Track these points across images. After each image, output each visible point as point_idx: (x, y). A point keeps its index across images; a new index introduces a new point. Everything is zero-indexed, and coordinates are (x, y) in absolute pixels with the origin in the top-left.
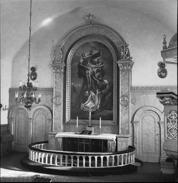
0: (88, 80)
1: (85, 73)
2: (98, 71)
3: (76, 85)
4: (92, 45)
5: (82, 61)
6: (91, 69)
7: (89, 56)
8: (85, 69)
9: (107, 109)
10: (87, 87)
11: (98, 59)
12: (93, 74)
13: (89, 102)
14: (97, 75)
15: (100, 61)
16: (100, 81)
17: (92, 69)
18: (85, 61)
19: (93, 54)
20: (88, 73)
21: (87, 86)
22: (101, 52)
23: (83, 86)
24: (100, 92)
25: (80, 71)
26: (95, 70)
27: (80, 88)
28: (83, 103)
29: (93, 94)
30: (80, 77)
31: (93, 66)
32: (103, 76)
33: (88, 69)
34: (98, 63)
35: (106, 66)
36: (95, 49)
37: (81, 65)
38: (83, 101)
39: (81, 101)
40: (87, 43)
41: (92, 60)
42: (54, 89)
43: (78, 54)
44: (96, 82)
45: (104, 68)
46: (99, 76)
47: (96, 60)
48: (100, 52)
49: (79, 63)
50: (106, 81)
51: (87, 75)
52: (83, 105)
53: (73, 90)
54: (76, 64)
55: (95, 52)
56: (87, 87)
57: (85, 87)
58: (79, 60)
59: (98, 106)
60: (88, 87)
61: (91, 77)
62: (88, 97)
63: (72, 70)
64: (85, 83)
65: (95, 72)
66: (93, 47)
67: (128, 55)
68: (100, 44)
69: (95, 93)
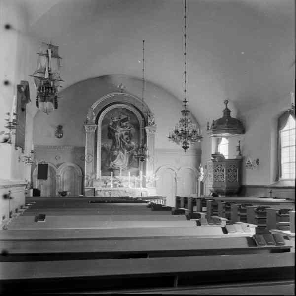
0: (117, 141)
1: (115, 135)
2: (126, 134)
3: (106, 146)
4: (121, 110)
5: (111, 124)
6: (120, 132)
7: (118, 120)
8: (114, 132)
9: (134, 167)
10: (116, 148)
11: (127, 124)
12: (122, 136)
13: (117, 161)
14: (125, 137)
15: (128, 125)
16: (128, 143)
17: (121, 131)
18: (115, 124)
19: (122, 119)
20: (117, 136)
21: (116, 146)
22: (129, 118)
23: (112, 147)
24: (128, 152)
25: (109, 134)
26: (124, 133)
27: (110, 148)
28: (113, 161)
29: (121, 153)
30: (109, 138)
31: (122, 129)
32: (130, 139)
33: (117, 132)
34: (126, 127)
35: (133, 130)
36: (124, 114)
37: (111, 127)
38: (112, 159)
39: (110, 159)
40: (117, 109)
41: (121, 124)
42: (86, 148)
43: (109, 116)
44: (125, 143)
45: (132, 132)
46: (127, 139)
47: (124, 124)
48: (128, 118)
49: (109, 125)
50: (133, 143)
51: (116, 137)
52: (112, 163)
53: (103, 149)
54: (106, 126)
55: (123, 117)
56: (116, 148)
57: (115, 147)
58: (109, 122)
59: (126, 165)
60: (117, 147)
61: (120, 138)
62: (116, 156)
63: (102, 131)
64: (115, 143)
65: (124, 134)
66: (122, 113)
67: (154, 123)
68: (128, 111)
69: (124, 153)
